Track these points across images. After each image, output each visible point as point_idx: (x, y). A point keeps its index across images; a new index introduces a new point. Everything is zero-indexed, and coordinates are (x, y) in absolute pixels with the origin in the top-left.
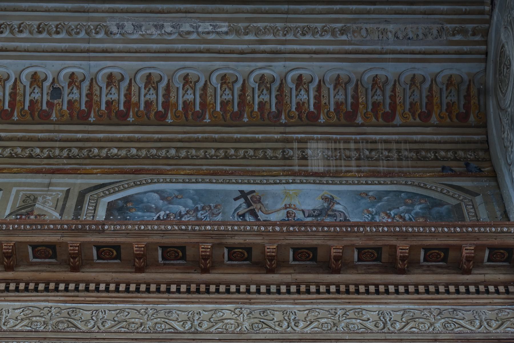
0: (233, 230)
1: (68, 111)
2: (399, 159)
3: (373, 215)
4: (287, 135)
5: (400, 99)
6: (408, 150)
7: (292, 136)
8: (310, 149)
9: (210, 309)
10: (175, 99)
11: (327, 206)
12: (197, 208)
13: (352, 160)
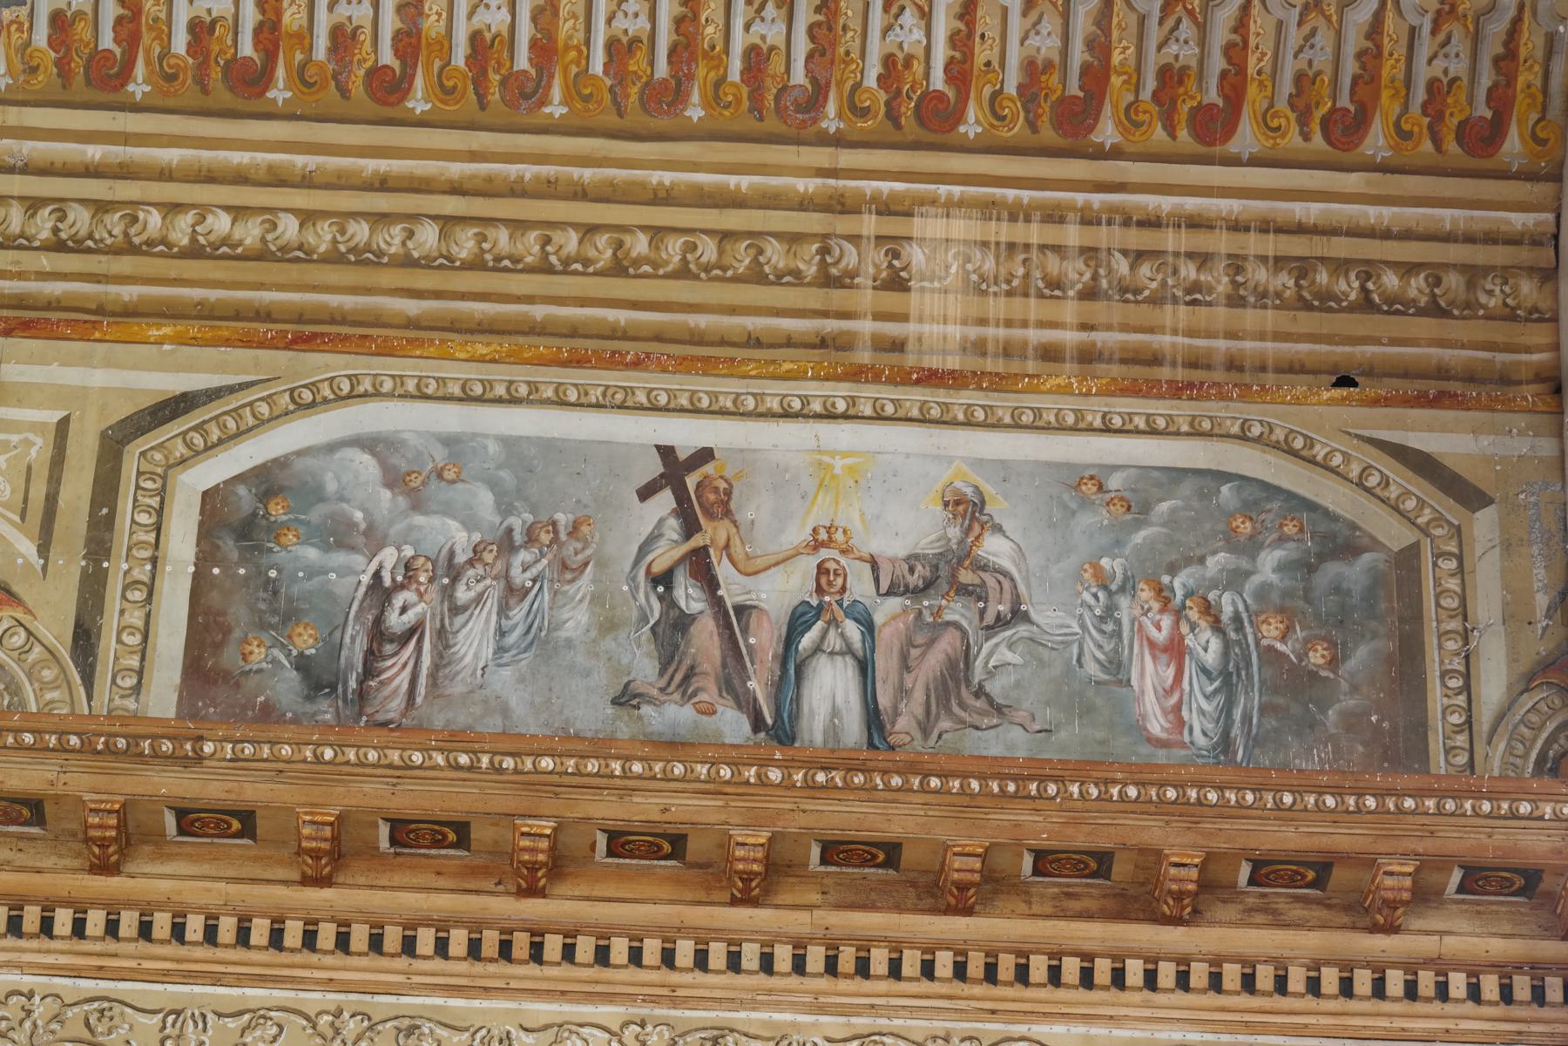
0: (626, 774)
1: (53, 54)
2: (1235, 301)
3: (1110, 594)
4: (841, 183)
5: (1260, 60)
6: (1271, 262)
7: (858, 188)
8: (922, 241)
9: (543, 1021)
10: (443, 23)
11: (961, 542)
12: (510, 531)
13: (1064, 298)
